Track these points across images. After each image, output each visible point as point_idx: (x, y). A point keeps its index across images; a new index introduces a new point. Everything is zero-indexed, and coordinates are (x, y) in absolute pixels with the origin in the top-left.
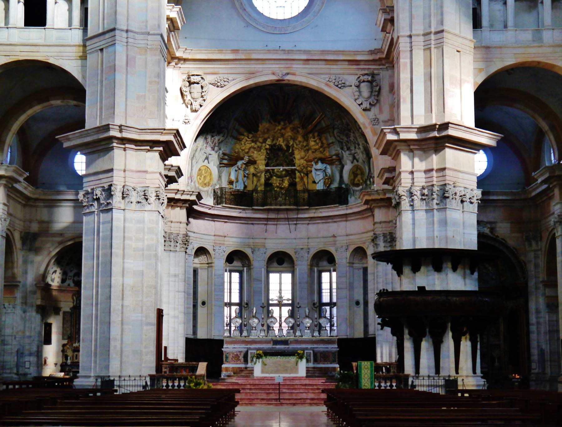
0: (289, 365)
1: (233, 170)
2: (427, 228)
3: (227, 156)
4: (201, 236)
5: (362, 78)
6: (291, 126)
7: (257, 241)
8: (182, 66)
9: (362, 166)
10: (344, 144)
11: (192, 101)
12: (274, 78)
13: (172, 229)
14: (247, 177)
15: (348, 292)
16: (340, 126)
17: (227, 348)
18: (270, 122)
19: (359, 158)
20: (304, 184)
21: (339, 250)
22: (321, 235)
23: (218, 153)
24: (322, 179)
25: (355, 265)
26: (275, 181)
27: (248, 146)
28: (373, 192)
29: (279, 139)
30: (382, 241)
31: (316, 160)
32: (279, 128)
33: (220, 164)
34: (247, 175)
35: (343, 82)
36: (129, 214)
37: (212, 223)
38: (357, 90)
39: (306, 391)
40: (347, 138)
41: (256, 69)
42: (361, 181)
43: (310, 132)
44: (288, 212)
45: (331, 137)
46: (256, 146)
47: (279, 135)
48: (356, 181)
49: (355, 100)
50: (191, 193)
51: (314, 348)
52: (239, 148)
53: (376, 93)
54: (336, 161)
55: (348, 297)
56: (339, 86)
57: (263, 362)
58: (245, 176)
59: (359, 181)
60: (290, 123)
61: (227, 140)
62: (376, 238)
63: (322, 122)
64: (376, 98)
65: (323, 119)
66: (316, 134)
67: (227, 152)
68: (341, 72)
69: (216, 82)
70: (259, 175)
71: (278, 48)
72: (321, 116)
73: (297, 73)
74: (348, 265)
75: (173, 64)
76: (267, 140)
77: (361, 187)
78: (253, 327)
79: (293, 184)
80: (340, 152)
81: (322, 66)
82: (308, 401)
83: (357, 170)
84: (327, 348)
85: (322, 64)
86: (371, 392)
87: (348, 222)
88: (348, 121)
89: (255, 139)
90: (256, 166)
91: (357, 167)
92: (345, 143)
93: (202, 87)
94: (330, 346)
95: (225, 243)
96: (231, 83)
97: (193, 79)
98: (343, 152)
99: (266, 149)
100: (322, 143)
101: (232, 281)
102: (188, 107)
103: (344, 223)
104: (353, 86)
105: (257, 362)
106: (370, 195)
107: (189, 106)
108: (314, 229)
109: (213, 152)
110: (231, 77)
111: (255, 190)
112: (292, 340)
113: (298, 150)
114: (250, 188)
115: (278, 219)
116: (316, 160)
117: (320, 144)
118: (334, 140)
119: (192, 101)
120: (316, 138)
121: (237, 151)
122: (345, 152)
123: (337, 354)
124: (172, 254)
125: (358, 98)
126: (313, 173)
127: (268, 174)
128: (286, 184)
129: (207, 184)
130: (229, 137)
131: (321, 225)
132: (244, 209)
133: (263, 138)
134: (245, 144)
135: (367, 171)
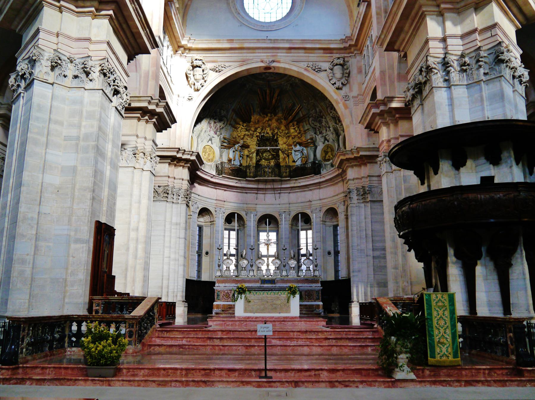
0: (279, 302)
1: (231, 151)
2: (470, 109)
4: (205, 199)
5: (336, 61)
6: (276, 118)
7: (249, 206)
8: (187, 55)
9: (332, 144)
10: (317, 130)
12: (262, 65)
13: (175, 185)
14: (242, 157)
15: (322, 245)
16: (314, 115)
17: (218, 287)
18: (260, 115)
19: (329, 139)
20: (286, 163)
21: (314, 211)
22: (299, 201)
25: (326, 223)
26: (263, 162)
27: (243, 133)
28: (348, 152)
29: (267, 128)
30: (355, 195)
32: (267, 119)
33: (222, 146)
35: (319, 67)
36: (59, 91)
37: (214, 190)
38: (331, 72)
39: (308, 343)
40: (320, 124)
41: (248, 58)
42: (331, 157)
43: (291, 122)
45: (306, 125)
46: (249, 134)
47: (267, 125)
49: (330, 80)
50: (191, 153)
51: (299, 286)
53: (347, 75)
55: (322, 248)
56: (316, 70)
57: (246, 299)
58: (240, 156)
59: (329, 156)
60: (275, 116)
61: (227, 126)
62: (350, 192)
63: (300, 112)
64: (347, 79)
65: (300, 110)
66: (295, 123)
67: (227, 136)
68: (318, 59)
70: (251, 156)
71: (266, 38)
72: (299, 107)
73: (282, 60)
74: (321, 222)
75: (180, 52)
77: (331, 161)
78: (243, 268)
79: (278, 165)
80: (314, 136)
81: (301, 54)
82: (325, 376)
83: (328, 149)
84: (311, 286)
86: (461, 358)
87: (321, 190)
88: (321, 108)
89: (248, 129)
90: (249, 149)
93: (203, 71)
94: (314, 285)
95: (225, 206)
96: (228, 69)
97: (196, 63)
99: (257, 136)
100: (300, 130)
101: (231, 237)
103: (318, 190)
104: (328, 70)
105: (239, 298)
106: (344, 155)
107: (193, 86)
108: (294, 197)
109: (215, 136)
110: (227, 64)
111: (248, 167)
112: (279, 279)
114: (244, 164)
115: (266, 189)
117: (298, 131)
118: (309, 127)
119: (195, 82)
120: (295, 127)
122: (318, 135)
123: (320, 292)
124: (174, 205)
125: (332, 79)
126: (293, 154)
128: (272, 163)
130: (228, 125)
131: (299, 194)
132: (239, 180)
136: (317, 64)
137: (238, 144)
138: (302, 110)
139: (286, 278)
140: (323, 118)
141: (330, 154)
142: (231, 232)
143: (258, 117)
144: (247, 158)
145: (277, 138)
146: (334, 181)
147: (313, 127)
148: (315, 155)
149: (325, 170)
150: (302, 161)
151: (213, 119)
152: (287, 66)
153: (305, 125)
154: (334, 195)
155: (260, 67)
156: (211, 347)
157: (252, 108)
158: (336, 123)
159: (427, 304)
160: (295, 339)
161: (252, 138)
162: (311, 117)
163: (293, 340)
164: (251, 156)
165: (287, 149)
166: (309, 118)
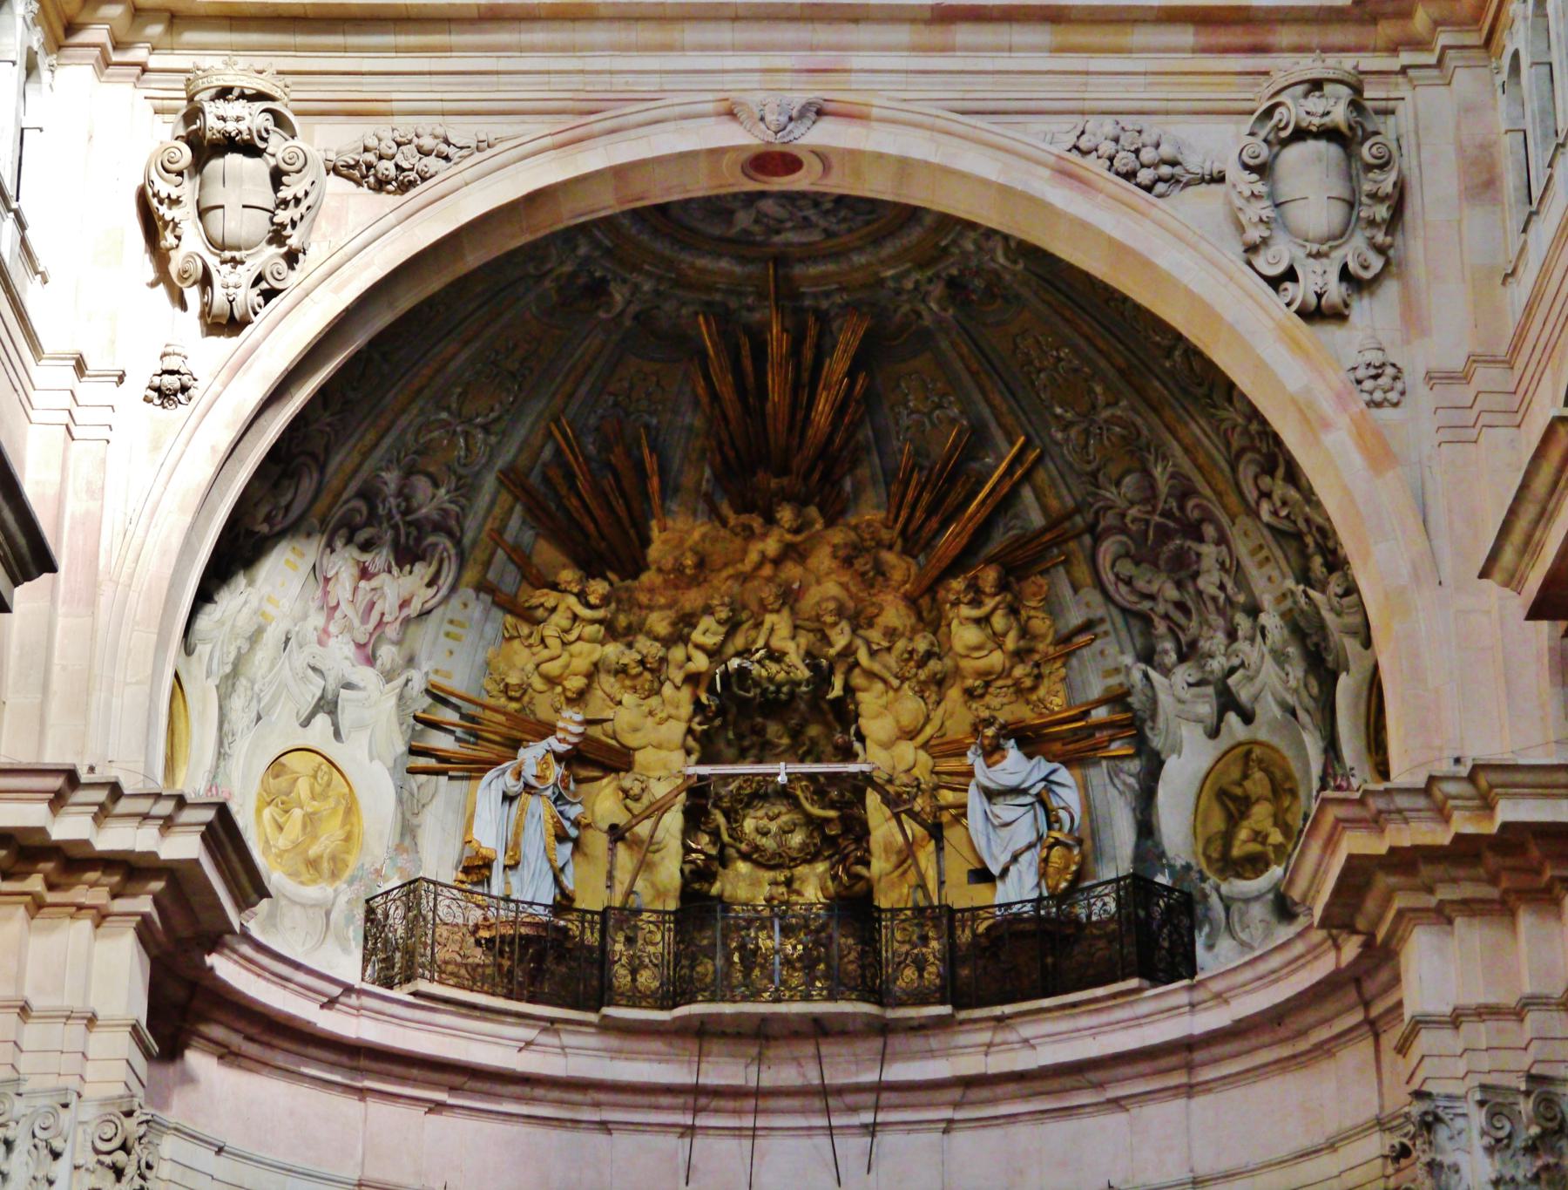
1: (489, 789)
3: (456, 708)
5: (1296, 110)
6: (838, 536)
9: (1279, 742)
10: (1161, 627)
11: (213, 262)
13: (25, 1063)
14: (577, 843)
18: (714, 513)
19: (1256, 698)
20: (922, 886)
23: (401, 680)
24: (1030, 846)
27: (585, 654)
28: (1402, 802)
29: (769, 619)
30: (1478, 1143)
31: (990, 732)
32: (771, 546)
33: (414, 751)
34: (573, 832)
35: (1166, 151)
37: (349, 1106)
38: (1260, 188)
40: (1179, 585)
41: (619, 82)
42: (1276, 837)
43: (955, 567)
44: (824, 1050)
45: (1076, 589)
46: (630, 657)
47: (769, 593)
48: (1242, 844)
49: (1252, 249)
50: (166, 807)
52: (530, 667)
53: (1382, 212)
54: (1112, 740)
56: (1145, 176)
58: (561, 837)
59: (1259, 836)
60: (830, 523)
61: (455, 602)
62: (1429, 1123)
63: (1027, 493)
64: (1380, 237)
65: (1028, 476)
66: (990, 576)
67: (459, 680)
69: (370, 157)
70: (643, 829)
72: (1022, 451)
73: (878, 103)
76: (694, 627)
77: (1276, 871)
80: (1136, 676)
83: (1245, 776)
85: (1034, 48)
87: (1200, 1102)
88: (1186, 466)
89: (622, 620)
90: (627, 781)
91: (1246, 756)
92: (1166, 617)
93: (277, 177)
96: (466, 168)
97: (220, 118)
98: (1153, 674)
99: (692, 679)
100: (1024, 633)
102: (183, 305)
103: (1176, 1106)
104: (1234, 173)
106: (1376, 823)
107: (193, 295)
109: (366, 676)
110: (462, 131)
111: (622, 917)
113: (880, 686)
114: (591, 898)
115: (759, 1093)
116: (990, 732)
117: (1011, 643)
119: (213, 262)
120: (990, 603)
121: (513, 680)
122: (1166, 672)
125: (1265, 241)
127: (705, 839)
128: (813, 886)
129: (326, 866)
130: (466, 593)
131: (1023, 1134)
133: (671, 614)
134: (564, 644)
135: (1316, 769)
136: (1153, 127)
137: (542, 737)
138: (1041, 476)
140: (1201, 539)
141: (1261, 814)
143: (698, 531)
144: (612, 851)
145: (849, 689)
146: (1302, 1033)
147: (1125, 611)
148: (1146, 828)
149: (1225, 944)
150: (1043, 874)
151: (349, 541)
152: (917, 146)
153: (1067, 591)
154: (1305, 1143)
155: (715, 153)
157: (650, 463)
158: (1304, 577)
161: (658, 692)
162: (1109, 531)
164: (643, 829)
165: (927, 780)
166: (1097, 540)
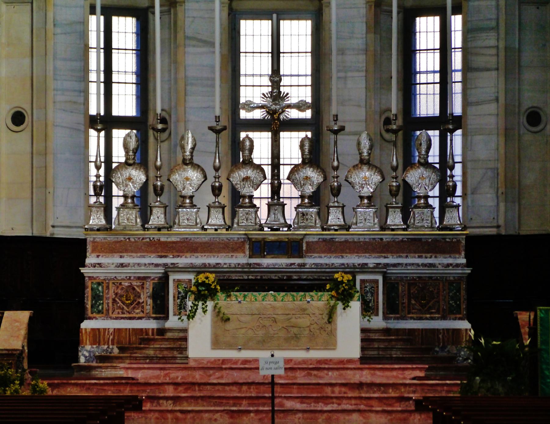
15: (502, 79)
39: (362, 407)
51: (386, 265)
57: (217, 311)
78: (184, 197)
84: (431, 265)
105: (200, 311)
112: (315, 239)
139: (341, 236)
142: (115, 20)
156: (157, 415)
159: (541, 325)
160: (334, 400)
163: (331, 401)
